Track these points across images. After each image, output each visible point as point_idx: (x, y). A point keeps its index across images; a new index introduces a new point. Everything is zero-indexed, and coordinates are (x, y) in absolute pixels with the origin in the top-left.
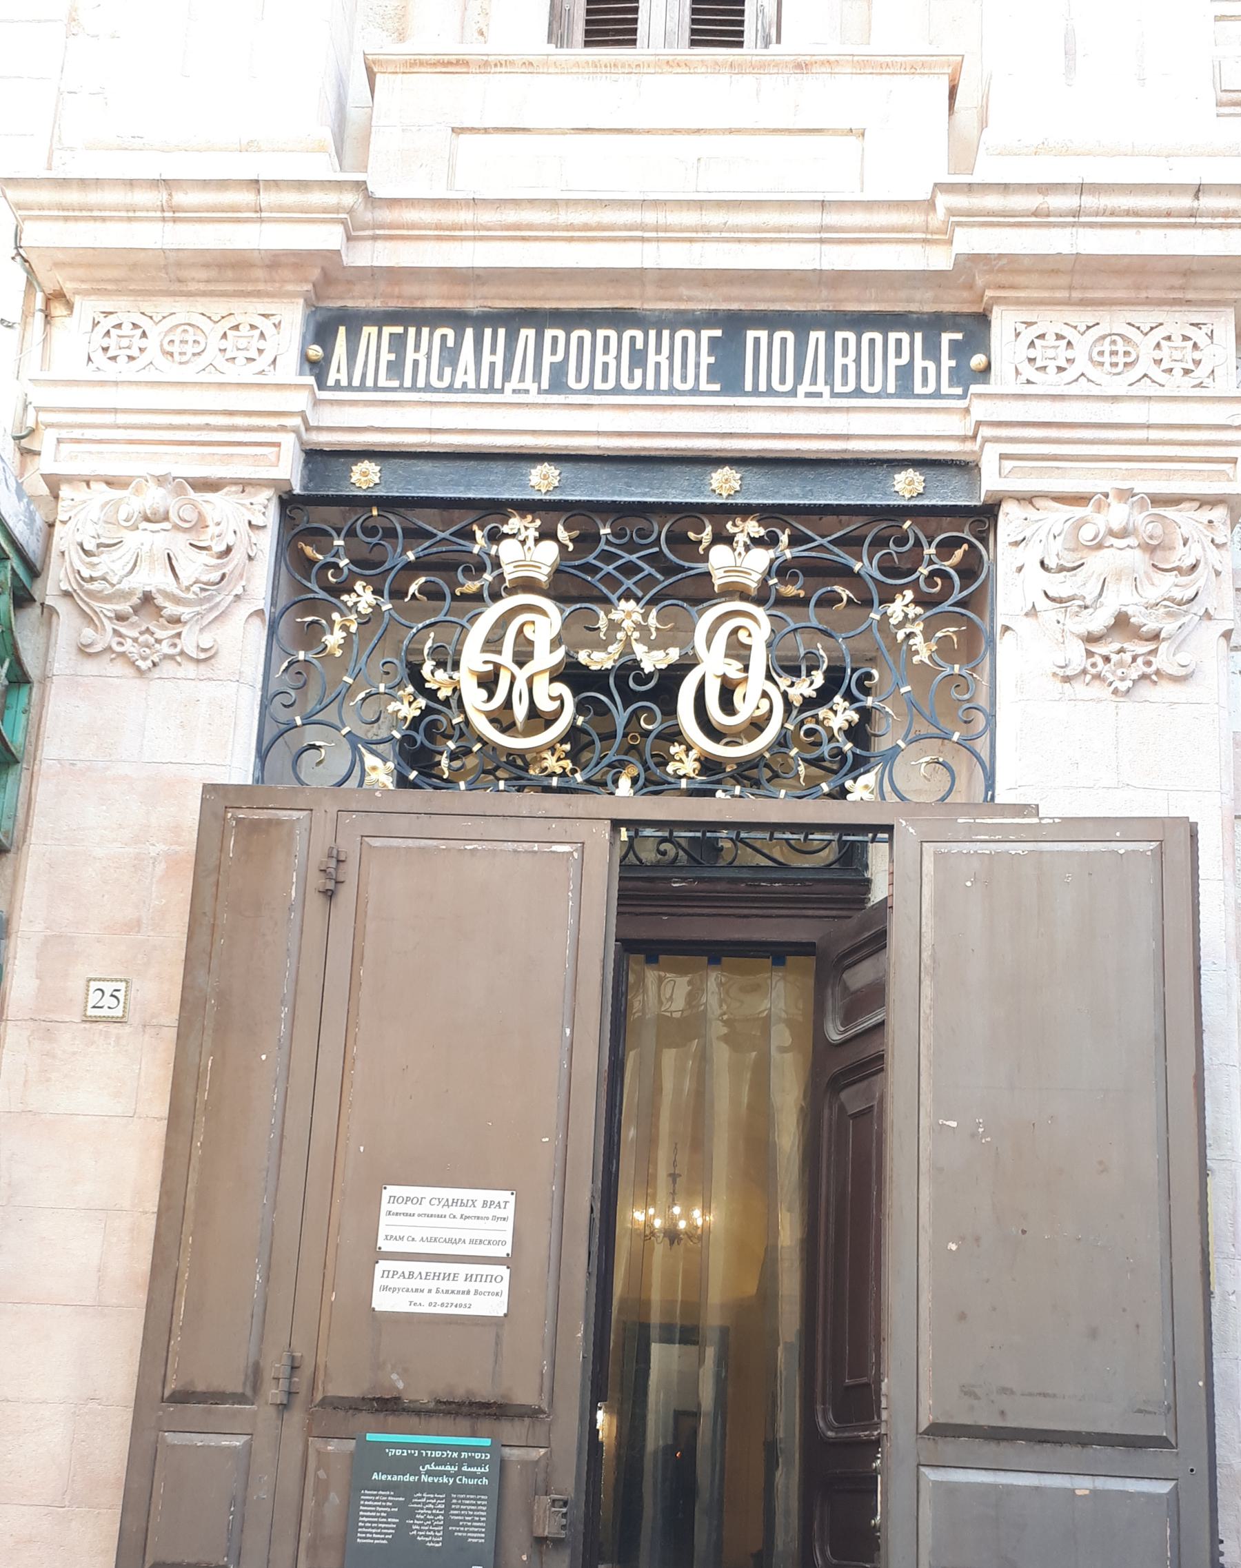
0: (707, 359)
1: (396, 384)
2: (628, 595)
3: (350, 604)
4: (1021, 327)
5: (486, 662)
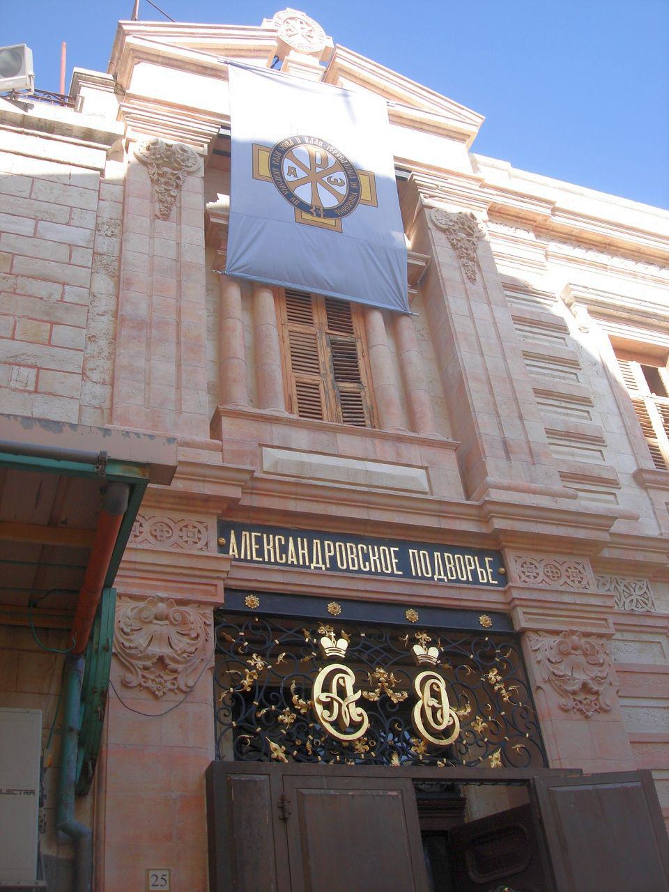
0: (394, 561)
1: (261, 560)
2: (380, 665)
3: (253, 664)
4: (517, 558)
5: (327, 697)
